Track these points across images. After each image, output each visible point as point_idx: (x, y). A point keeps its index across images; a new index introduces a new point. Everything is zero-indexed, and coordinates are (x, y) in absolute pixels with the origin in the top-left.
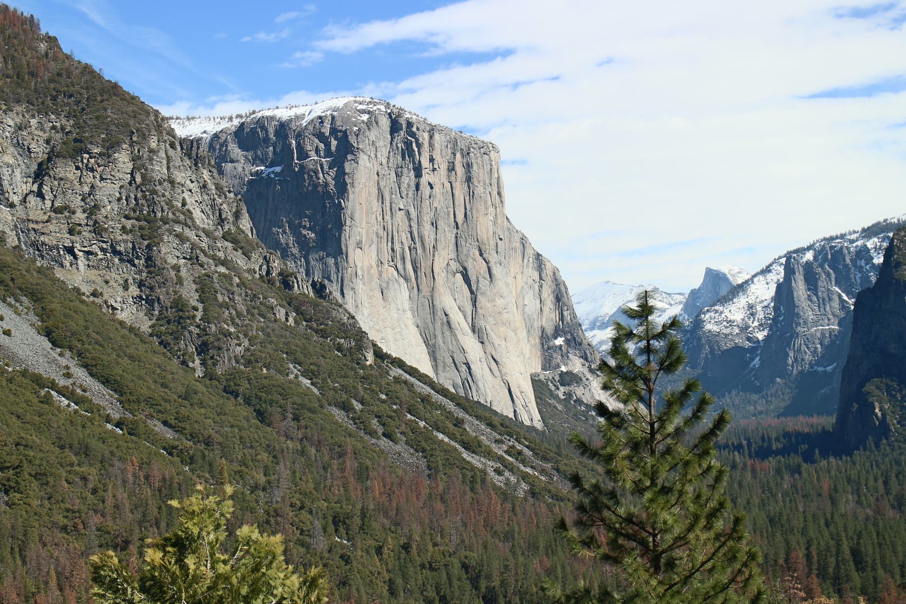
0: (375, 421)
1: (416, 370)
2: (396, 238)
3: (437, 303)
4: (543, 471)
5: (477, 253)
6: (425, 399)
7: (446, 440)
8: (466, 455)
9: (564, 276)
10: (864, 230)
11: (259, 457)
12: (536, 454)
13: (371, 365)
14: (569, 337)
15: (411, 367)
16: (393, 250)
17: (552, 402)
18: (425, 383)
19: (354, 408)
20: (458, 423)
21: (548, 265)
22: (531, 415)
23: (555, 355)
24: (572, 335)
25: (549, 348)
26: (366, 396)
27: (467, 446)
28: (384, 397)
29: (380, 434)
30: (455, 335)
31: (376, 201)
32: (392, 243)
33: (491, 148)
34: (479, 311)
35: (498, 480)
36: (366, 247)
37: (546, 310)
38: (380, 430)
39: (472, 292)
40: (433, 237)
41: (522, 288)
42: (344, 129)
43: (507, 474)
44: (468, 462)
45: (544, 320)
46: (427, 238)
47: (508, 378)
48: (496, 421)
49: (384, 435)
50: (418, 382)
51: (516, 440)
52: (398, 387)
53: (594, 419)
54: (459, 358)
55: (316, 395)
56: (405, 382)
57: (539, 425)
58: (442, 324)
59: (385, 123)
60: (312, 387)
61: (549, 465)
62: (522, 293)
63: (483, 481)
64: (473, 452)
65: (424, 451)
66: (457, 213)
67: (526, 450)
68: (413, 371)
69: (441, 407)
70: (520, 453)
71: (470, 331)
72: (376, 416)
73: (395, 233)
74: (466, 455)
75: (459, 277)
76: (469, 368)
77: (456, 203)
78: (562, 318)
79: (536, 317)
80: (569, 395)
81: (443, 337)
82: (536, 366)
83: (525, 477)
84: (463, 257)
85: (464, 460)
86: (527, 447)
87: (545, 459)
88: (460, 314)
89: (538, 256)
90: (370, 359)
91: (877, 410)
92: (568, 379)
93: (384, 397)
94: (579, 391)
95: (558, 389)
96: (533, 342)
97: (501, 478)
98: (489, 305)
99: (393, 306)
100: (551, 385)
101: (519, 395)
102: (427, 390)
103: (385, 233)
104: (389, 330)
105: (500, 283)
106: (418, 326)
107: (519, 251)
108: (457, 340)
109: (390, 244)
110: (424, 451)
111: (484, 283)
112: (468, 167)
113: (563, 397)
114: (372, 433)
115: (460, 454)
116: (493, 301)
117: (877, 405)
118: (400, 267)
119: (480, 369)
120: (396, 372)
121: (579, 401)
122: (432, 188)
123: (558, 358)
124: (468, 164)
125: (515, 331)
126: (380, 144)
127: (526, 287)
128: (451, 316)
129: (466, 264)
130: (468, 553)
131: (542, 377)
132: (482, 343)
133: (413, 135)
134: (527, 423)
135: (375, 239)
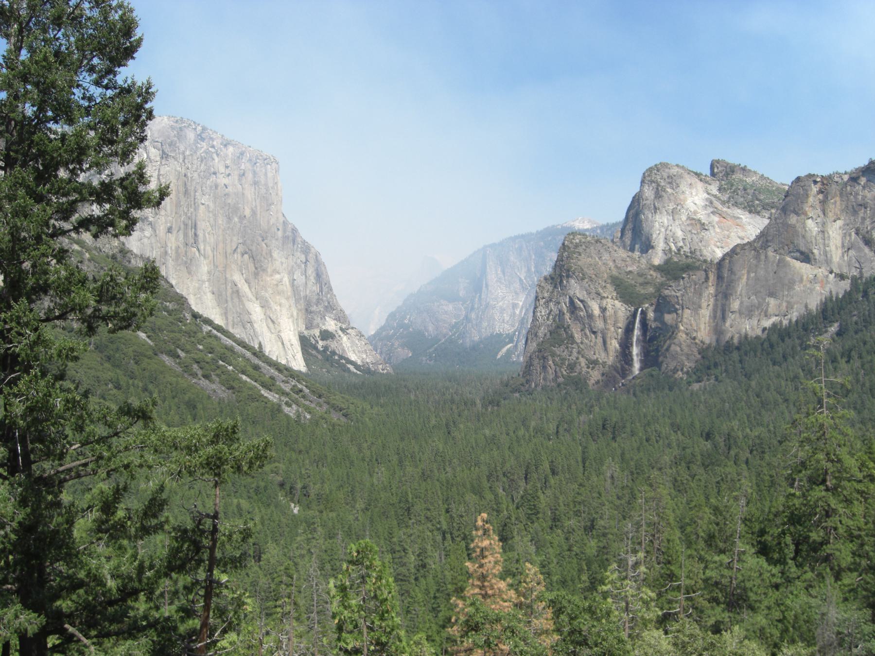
0: (195, 366)
1: (221, 327)
5: (260, 239)
6: (231, 349)
7: (248, 380)
8: (264, 392)
9: (323, 258)
11: (111, 392)
12: (313, 392)
14: (326, 304)
17: (314, 352)
18: (229, 337)
19: (178, 356)
20: (256, 368)
21: (313, 250)
22: (298, 364)
23: (315, 317)
25: (311, 312)
27: (264, 385)
28: (201, 347)
29: (200, 376)
35: (291, 411)
36: (175, 232)
37: (310, 284)
38: (200, 373)
39: (256, 268)
41: (293, 267)
42: (160, 140)
43: (294, 406)
44: (266, 397)
45: (308, 292)
47: (282, 335)
48: (282, 368)
50: (223, 337)
51: (298, 381)
52: (209, 340)
53: (344, 366)
54: (246, 318)
55: (151, 346)
56: (216, 337)
58: (233, 292)
59: (191, 135)
60: (148, 340)
63: (279, 409)
64: (270, 390)
65: (231, 388)
68: (219, 328)
69: (244, 357)
70: (301, 391)
71: (254, 299)
72: (198, 362)
74: (264, 392)
76: (252, 326)
78: (321, 291)
80: (326, 348)
82: (302, 328)
84: (248, 242)
87: (320, 397)
88: (246, 285)
89: (304, 242)
92: (326, 335)
93: (201, 347)
94: (333, 345)
97: (289, 409)
99: (195, 278)
102: (229, 342)
107: (291, 238)
108: (244, 305)
112: (255, 173)
114: (195, 375)
116: (271, 275)
117: (550, 358)
118: (202, 247)
120: (207, 328)
121: (334, 353)
123: (318, 320)
125: (287, 298)
126: (188, 153)
130: (277, 464)
131: (306, 333)
133: (213, 147)
134: (296, 368)
135: (182, 227)
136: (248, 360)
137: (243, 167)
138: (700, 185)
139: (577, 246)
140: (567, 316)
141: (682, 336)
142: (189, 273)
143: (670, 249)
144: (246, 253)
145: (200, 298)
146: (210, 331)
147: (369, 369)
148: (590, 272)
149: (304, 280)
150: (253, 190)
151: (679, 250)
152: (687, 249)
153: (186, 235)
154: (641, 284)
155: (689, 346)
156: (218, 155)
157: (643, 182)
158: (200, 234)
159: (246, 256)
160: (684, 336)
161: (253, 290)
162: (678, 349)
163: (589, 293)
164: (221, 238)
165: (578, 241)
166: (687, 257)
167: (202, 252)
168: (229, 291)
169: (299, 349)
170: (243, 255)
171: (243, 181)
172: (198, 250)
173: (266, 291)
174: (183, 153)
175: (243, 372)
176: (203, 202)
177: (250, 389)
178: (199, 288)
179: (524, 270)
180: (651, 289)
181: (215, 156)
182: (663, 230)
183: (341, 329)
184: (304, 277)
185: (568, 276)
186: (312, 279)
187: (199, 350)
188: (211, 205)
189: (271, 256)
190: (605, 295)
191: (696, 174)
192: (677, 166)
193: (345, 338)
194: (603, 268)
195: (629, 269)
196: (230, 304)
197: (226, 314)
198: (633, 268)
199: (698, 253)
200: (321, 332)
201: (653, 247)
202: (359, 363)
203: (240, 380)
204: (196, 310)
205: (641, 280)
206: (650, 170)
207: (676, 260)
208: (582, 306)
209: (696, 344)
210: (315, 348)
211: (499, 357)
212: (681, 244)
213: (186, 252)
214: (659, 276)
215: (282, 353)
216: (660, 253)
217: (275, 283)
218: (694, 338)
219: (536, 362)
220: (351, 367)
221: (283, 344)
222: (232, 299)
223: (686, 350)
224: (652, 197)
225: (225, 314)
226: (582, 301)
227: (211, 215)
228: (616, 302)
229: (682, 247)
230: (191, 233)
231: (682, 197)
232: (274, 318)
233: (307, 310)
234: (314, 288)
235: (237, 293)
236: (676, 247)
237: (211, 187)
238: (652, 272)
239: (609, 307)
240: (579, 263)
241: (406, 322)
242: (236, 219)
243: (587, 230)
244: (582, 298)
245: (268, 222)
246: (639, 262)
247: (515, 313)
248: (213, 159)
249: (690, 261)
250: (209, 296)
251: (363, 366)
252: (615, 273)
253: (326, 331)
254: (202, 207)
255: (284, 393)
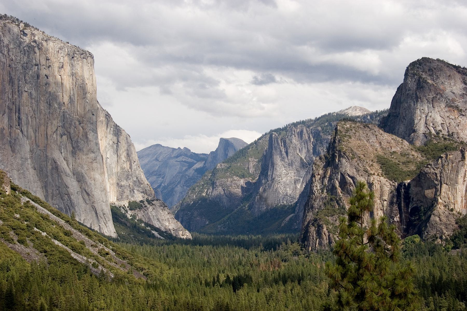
0: (12, 233)
2: (22, 111)
3: (49, 154)
4: (123, 266)
5: (77, 123)
6: (46, 218)
7: (60, 245)
10: (317, 119)
13: (8, 195)
14: (135, 179)
15: (36, 197)
16: (19, 118)
20: (67, 234)
23: (126, 190)
24: (137, 178)
26: (6, 215)
28: (18, 216)
30: (61, 176)
31: (7, 84)
32: (19, 113)
33: (88, 55)
34: (78, 161)
38: (16, 238)
39: (73, 148)
40: (47, 111)
41: (106, 147)
44: (75, 260)
46: (43, 112)
47: (96, 205)
48: (91, 233)
49: (19, 241)
50: (39, 207)
53: (150, 232)
57: (114, 235)
58: (52, 168)
61: (125, 261)
62: (106, 150)
66: (65, 96)
67: (111, 252)
68: (36, 200)
69: (57, 224)
70: (107, 254)
71: (71, 174)
73: (22, 108)
74: (74, 255)
75: (65, 137)
77: (64, 89)
78: (131, 168)
79: (114, 166)
80: (134, 217)
81: (52, 177)
83: (111, 268)
84: (67, 125)
85: (73, 258)
86: (113, 250)
88: (65, 163)
89: (116, 126)
90: (8, 191)
91: (325, 229)
95: (127, 212)
96: (111, 182)
97: (96, 270)
98: (84, 157)
99: (18, 155)
100: (122, 210)
101: (102, 216)
103: (14, 107)
104: (15, 172)
105: (92, 143)
106: (35, 169)
107: (104, 123)
109: (17, 114)
110: (45, 252)
111: (81, 144)
113: (130, 218)
115: (70, 254)
116: (87, 154)
117: (324, 226)
118: (25, 129)
119: (77, 199)
120: (24, 199)
122: (48, 78)
124: (72, 65)
126: (11, 46)
127: (108, 146)
128: (59, 163)
129: (69, 130)
131: (117, 204)
132: (79, 181)
134: (107, 234)
135: (7, 110)
136: (61, 227)
137: (62, 60)
138: (458, 76)
139: (347, 130)
140: (339, 190)
141: (440, 208)
142: (13, 151)
143: (430, 132)
144: (65, 134)
145: (23, 173)
146: (28, 202)
147: (171, 235)
148: (359, 153)
149: (116, 159)
150: (71, 80)
151: (438, 133)
152: (445, 132)
153: (10, 118)
154: (404, 163)
155: (447, 217)
156: (39, 49)
157: (406, 75)
158: (23, 117)
159: (65, 137)
160: (442, 207)
161: (71, 166)
162: (437, 219)
163: (358, 171)
164: (43, 121)
165: (348, 126)
166: (445, 139)
167: (26, 133)
168: (50, 167)
169: (111, 217)
170: (61, 136)
171: (62, 73)
172: (22, 131)
173: (82, 167)
174: (7, 46)
175: (56, 238)
176: (26, 89)
177: (62, 252)
178: (22, 165)
179: (304, 151)
180: (413, 167)
181: (36, 49)
182: (424, 116)
183: (147, 200)
184: (116, 156)
185: (340, 156)
186: (123, 158)
187: (16, 218)
188: (33, 92)
189: (87, 138)
190: (372, 172)
191: (455, 67)
192: (438, 60)
193: (151, 208)
194: (371, 149)
195: (393, 150)
196: (50, 178)
197: (46, 187)
198: (398, 149)
199: (455, 136)
200: (129, 202)
201: (414, 131)
202: (163, 229)
203: (52, 245)
204: (16, 183)
205: (404, 159)
206: (413, 65)
207: (435, 142)
208: (352, 182)
209: (453, 214)
210: (125, 216)
211: (283, 225)
212: (440, 128)
213: (10, 133)
214: (420, 156)
215: (96, 221)
216: (421, 136)
217: (90, 161)
218: (452, 210)
219: (313, 229)
220: (156, 233)
221: (96, 213)
222: (52, 174)
223: (444, 219)
224: (415, 88)
225: (45, 187)
226: (352, 178)
227: (33, 101)
228: (382, 178)
229: (441, 131)
230: (15, 117)
231: (441, 87)
232: (89, 191)
233: (118, 184)
234: (125, 165)
235: (56, 168)
236: (436, 131)
237: (33, 77)
238: (413, 153)
239: (376, 182)
240: (350, 145)
241: (204, 194)
242: (56, 106)
243: (358, 117)
244: (351, 174)
245: (85, 108)
246: (402, 144)
247: (296, 188)
248: (35, 53)
249: (447, 142)
250: (32, 171)
251: (166, 232)
252: (381, 153)
253: (135, 202)
254: (25, 94)
255: (92, 256)
